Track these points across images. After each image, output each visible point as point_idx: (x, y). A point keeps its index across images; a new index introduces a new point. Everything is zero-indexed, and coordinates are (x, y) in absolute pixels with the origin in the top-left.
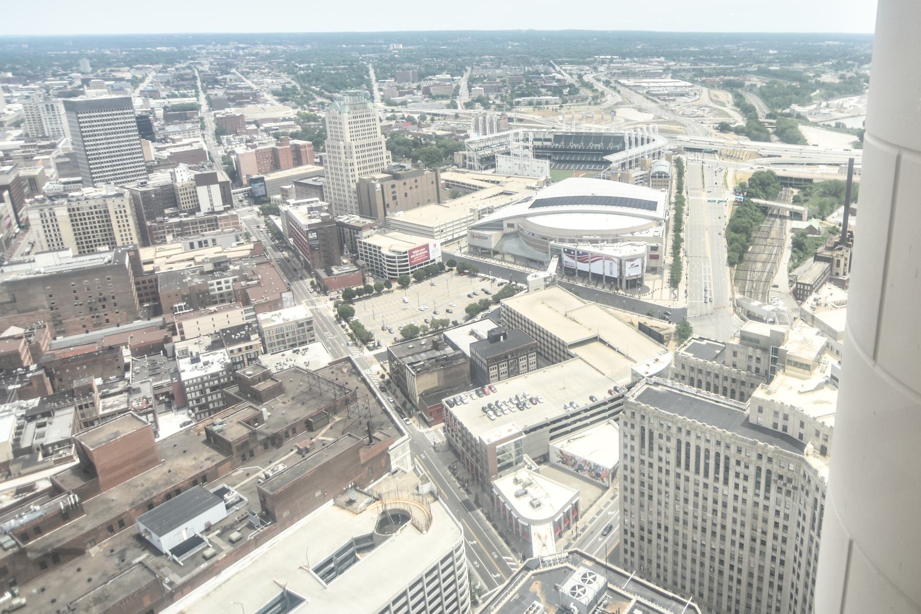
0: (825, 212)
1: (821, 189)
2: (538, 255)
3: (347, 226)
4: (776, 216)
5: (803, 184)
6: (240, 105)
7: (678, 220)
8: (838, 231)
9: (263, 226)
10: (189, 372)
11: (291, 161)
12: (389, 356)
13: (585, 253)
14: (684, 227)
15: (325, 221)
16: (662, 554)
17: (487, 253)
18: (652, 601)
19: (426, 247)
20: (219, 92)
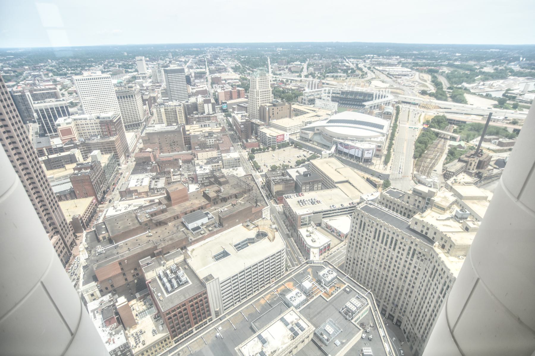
0: (469, 139)
1: (470, 127)
2: (328, 143)
3: (255, 124)
4: (442, 138)
5: (461, 124)
6: (220, 72)
7: (393, 135)
8: (474, 148)
9: (225, 121)
10: (199, 171)
11: (236, 96)
12: (266, 176)
13: (348, 145)
14: (395, 138)
15: (247, 121)
16: (361, 271)
17: (307, 140)
18: (354, 287)
19: (283, 135)
20: (213, 67)
